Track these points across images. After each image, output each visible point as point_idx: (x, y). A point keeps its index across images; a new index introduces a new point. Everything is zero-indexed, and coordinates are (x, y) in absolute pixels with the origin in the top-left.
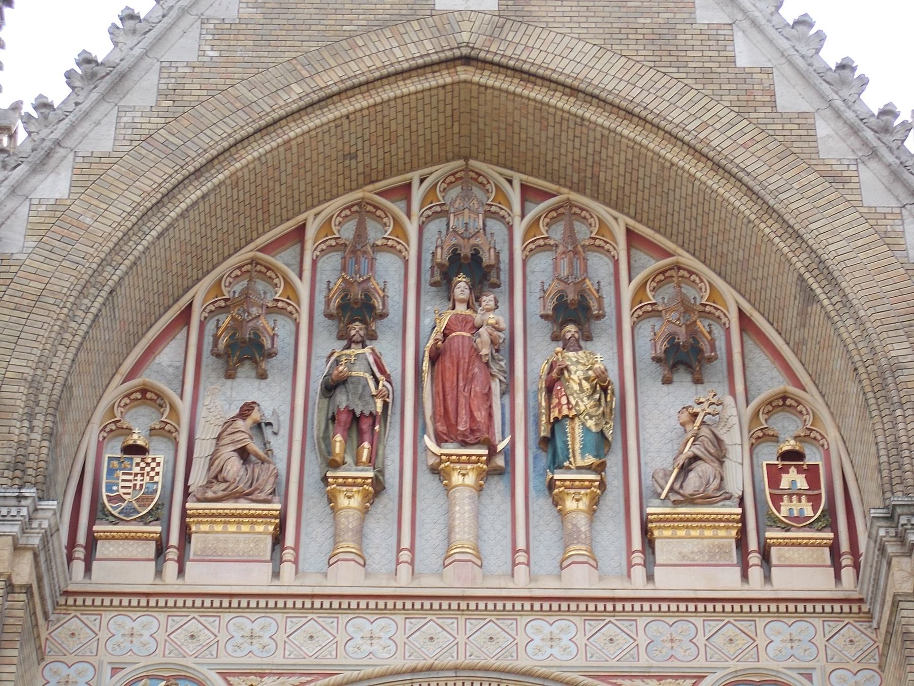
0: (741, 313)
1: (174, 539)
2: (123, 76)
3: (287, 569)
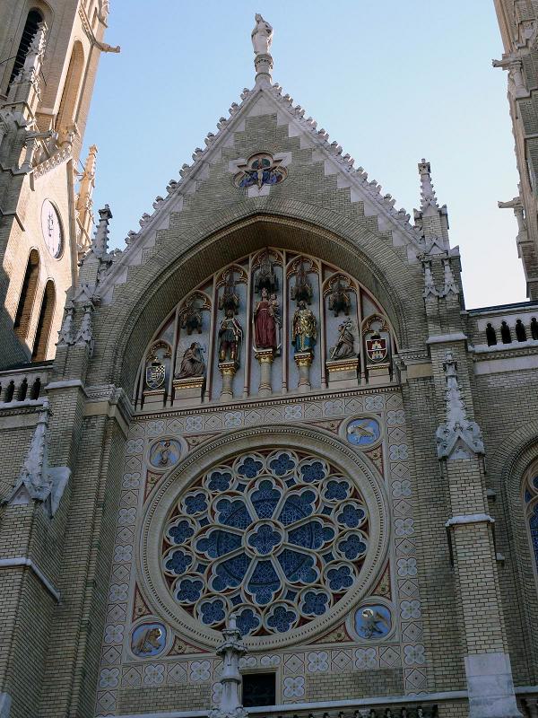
0: (360, 288)
1: (170, 394)
2: (144, 237)
3: (206, 399)
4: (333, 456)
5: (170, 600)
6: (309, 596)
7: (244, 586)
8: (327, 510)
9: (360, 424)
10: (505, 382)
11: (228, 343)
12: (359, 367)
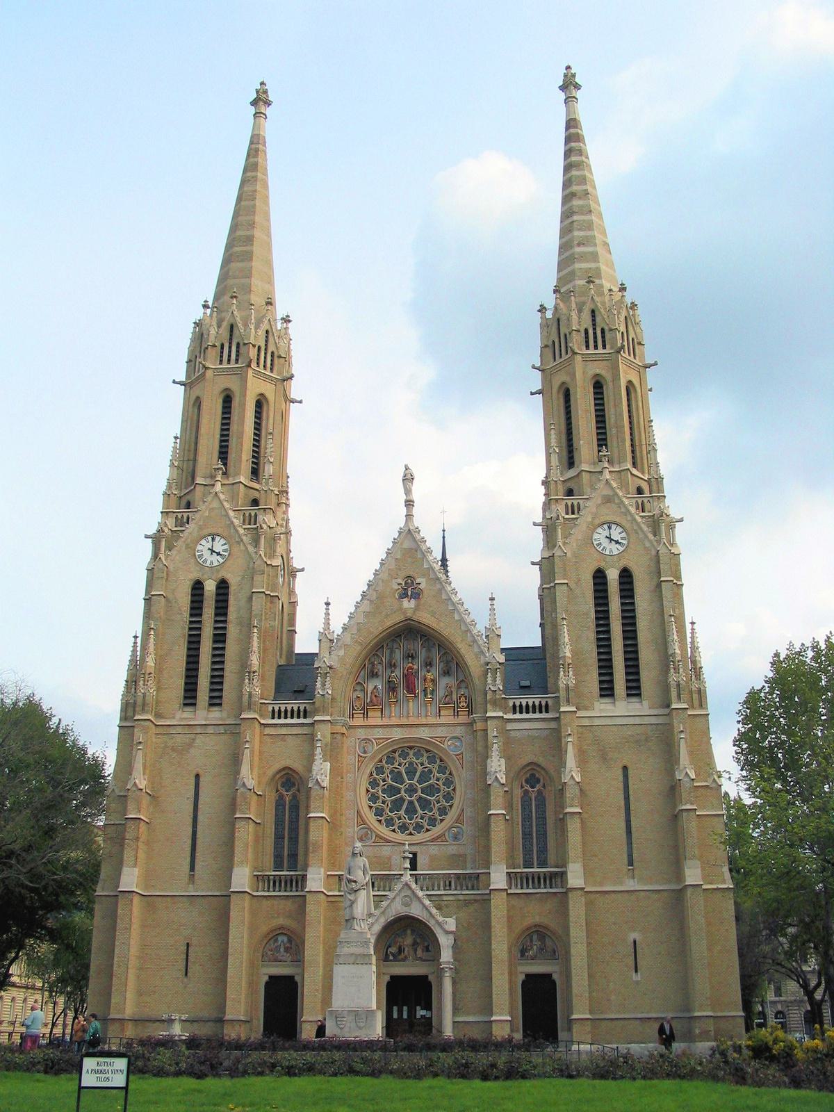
4: (441, 755)
5: (371, 818)
6: (430, 818)
7: (402, 812)
8: (438, 780)
9: (454, 740)
10: (518, 734)
11: (392, 688)
12: (454, 710)
